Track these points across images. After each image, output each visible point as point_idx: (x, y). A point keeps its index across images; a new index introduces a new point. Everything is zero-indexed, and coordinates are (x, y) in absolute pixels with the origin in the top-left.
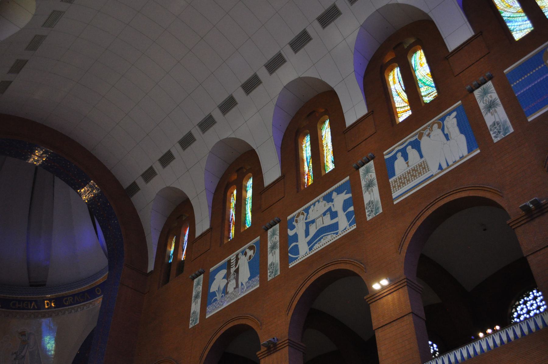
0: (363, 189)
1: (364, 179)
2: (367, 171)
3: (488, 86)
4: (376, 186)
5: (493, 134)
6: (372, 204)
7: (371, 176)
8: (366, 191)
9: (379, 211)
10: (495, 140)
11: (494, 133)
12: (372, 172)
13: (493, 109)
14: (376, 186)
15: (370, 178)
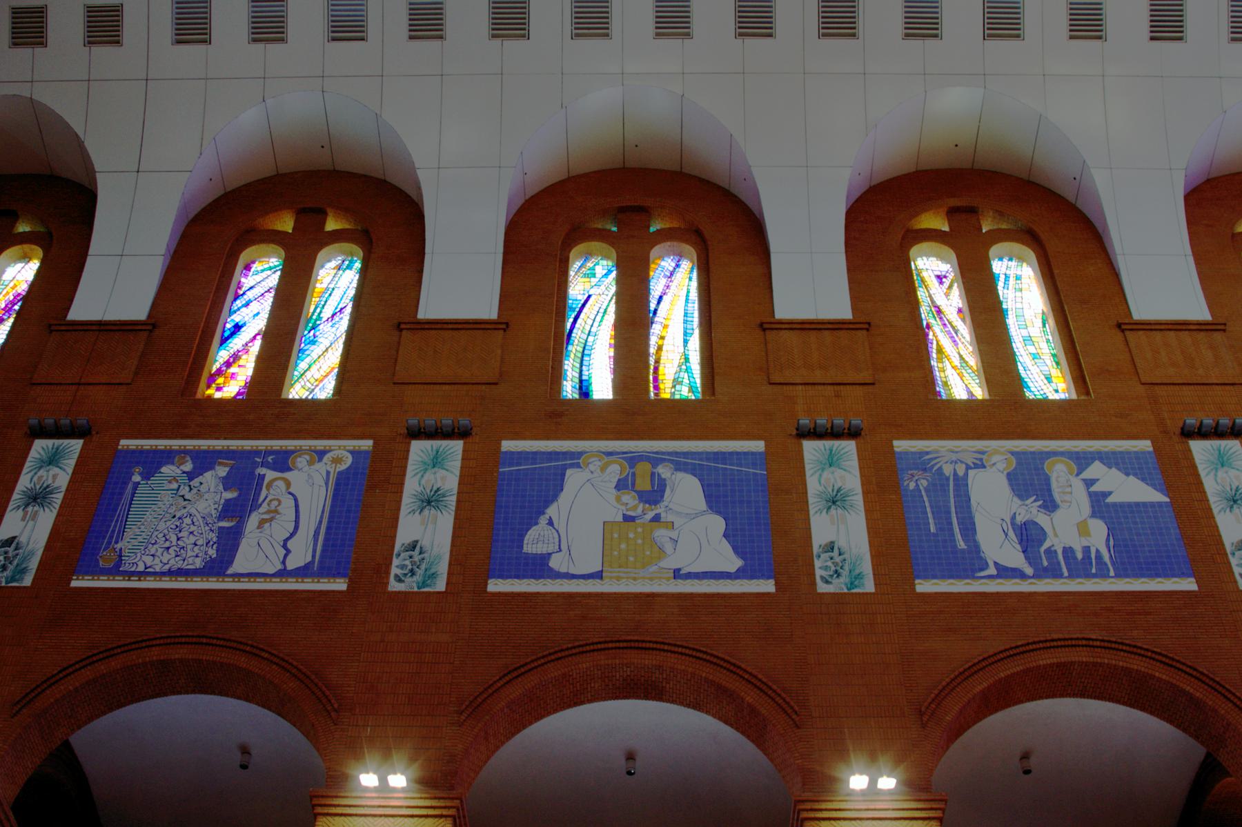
0: (15, 496)
1: (33, 473)
2: (53, 460)
3: (452, 450)
4: (51, 511)
5: (397, 567)
6: (16, 549)
7: (55, 477)
8: (18, 507)
9: (23, 579)
10: (394, 586)
11: (403, 567)
12: (64, 470)
13: (36, 508)
14: (51, 511)
15: (50, 481)
